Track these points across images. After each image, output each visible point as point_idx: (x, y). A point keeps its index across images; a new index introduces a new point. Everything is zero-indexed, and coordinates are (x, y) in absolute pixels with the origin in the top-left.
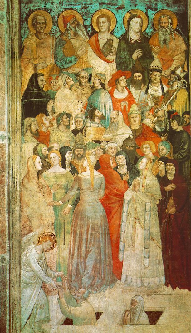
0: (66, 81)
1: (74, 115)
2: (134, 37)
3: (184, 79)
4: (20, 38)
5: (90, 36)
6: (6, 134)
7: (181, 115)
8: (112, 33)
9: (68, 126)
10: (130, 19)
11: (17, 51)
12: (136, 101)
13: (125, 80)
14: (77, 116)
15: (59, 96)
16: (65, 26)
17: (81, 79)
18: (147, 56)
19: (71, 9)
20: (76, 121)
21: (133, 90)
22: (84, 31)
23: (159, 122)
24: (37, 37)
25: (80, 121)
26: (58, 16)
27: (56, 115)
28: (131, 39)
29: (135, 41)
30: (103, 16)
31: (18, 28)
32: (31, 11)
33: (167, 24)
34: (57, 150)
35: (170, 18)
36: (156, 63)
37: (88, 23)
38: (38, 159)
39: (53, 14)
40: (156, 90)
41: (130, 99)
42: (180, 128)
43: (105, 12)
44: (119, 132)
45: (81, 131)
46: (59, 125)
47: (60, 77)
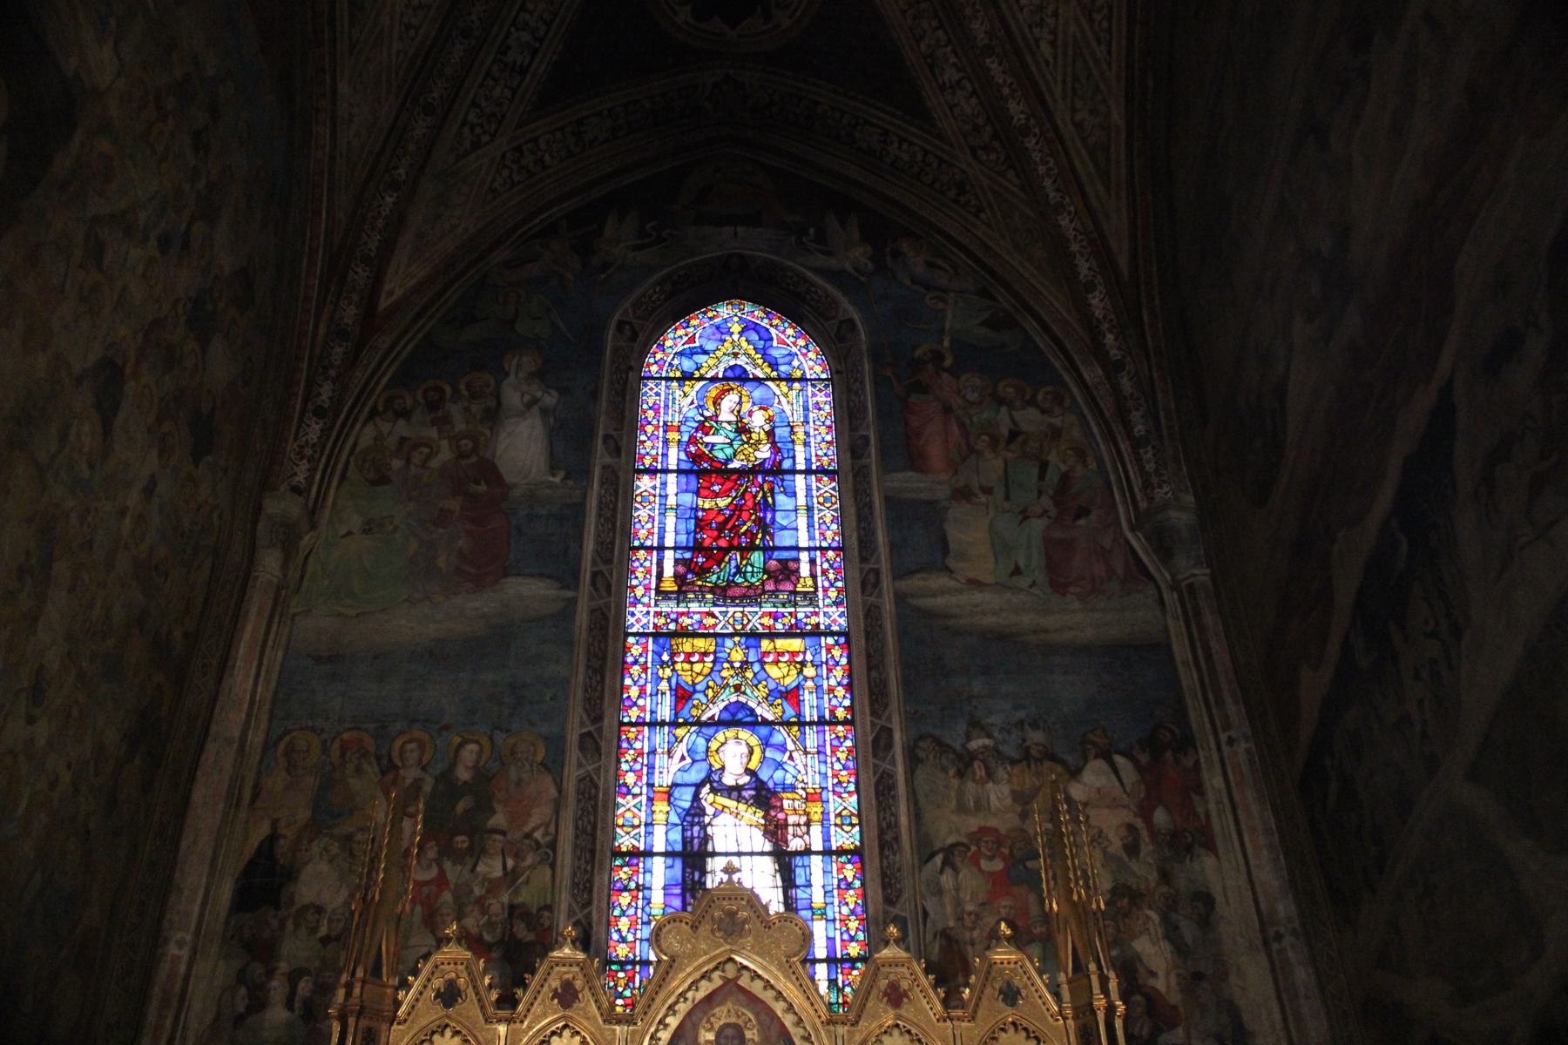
0: (325, 849)
1: (329, 909)
2: (463, 774)
3: (548, 847)
4: (259, 773)
5: (383, 773)
6: (189, 938)
7: (534, 911)
8: (424, 769)
9: (314, 930)
10: (461, 746)
11: (247, 795)
12: (452, 886)
13: (436, 849)
14: (334, 911)
15: (307, 873)
16: (343, 755)
17: (355, 846)
18: (484, 806)
19: (359, 729)
20: (330, 921)
21: (448, 865)
22: (375, 765)
23: (490, 925)
24: (287, 770)
25: (339, 921)
26: (333, 740)
27: (294, 910)
28: (457, 779)
29: (465, 782)
30: (410, 741)
31: (258, 757)
32: (287, 732)
33: (525, 755)
34: (283, 974)
35: (533, 745)
36: (498, 819)
37: (384, 752)
38: (243, 991)
39: (325, 736)
40: (492, 867)
41: (441, 881)
42: (531, 937)
43: (417, 733)
44: (413, 941)
45: (338, 939)
46: (297, 926)
47: (315, 843)
